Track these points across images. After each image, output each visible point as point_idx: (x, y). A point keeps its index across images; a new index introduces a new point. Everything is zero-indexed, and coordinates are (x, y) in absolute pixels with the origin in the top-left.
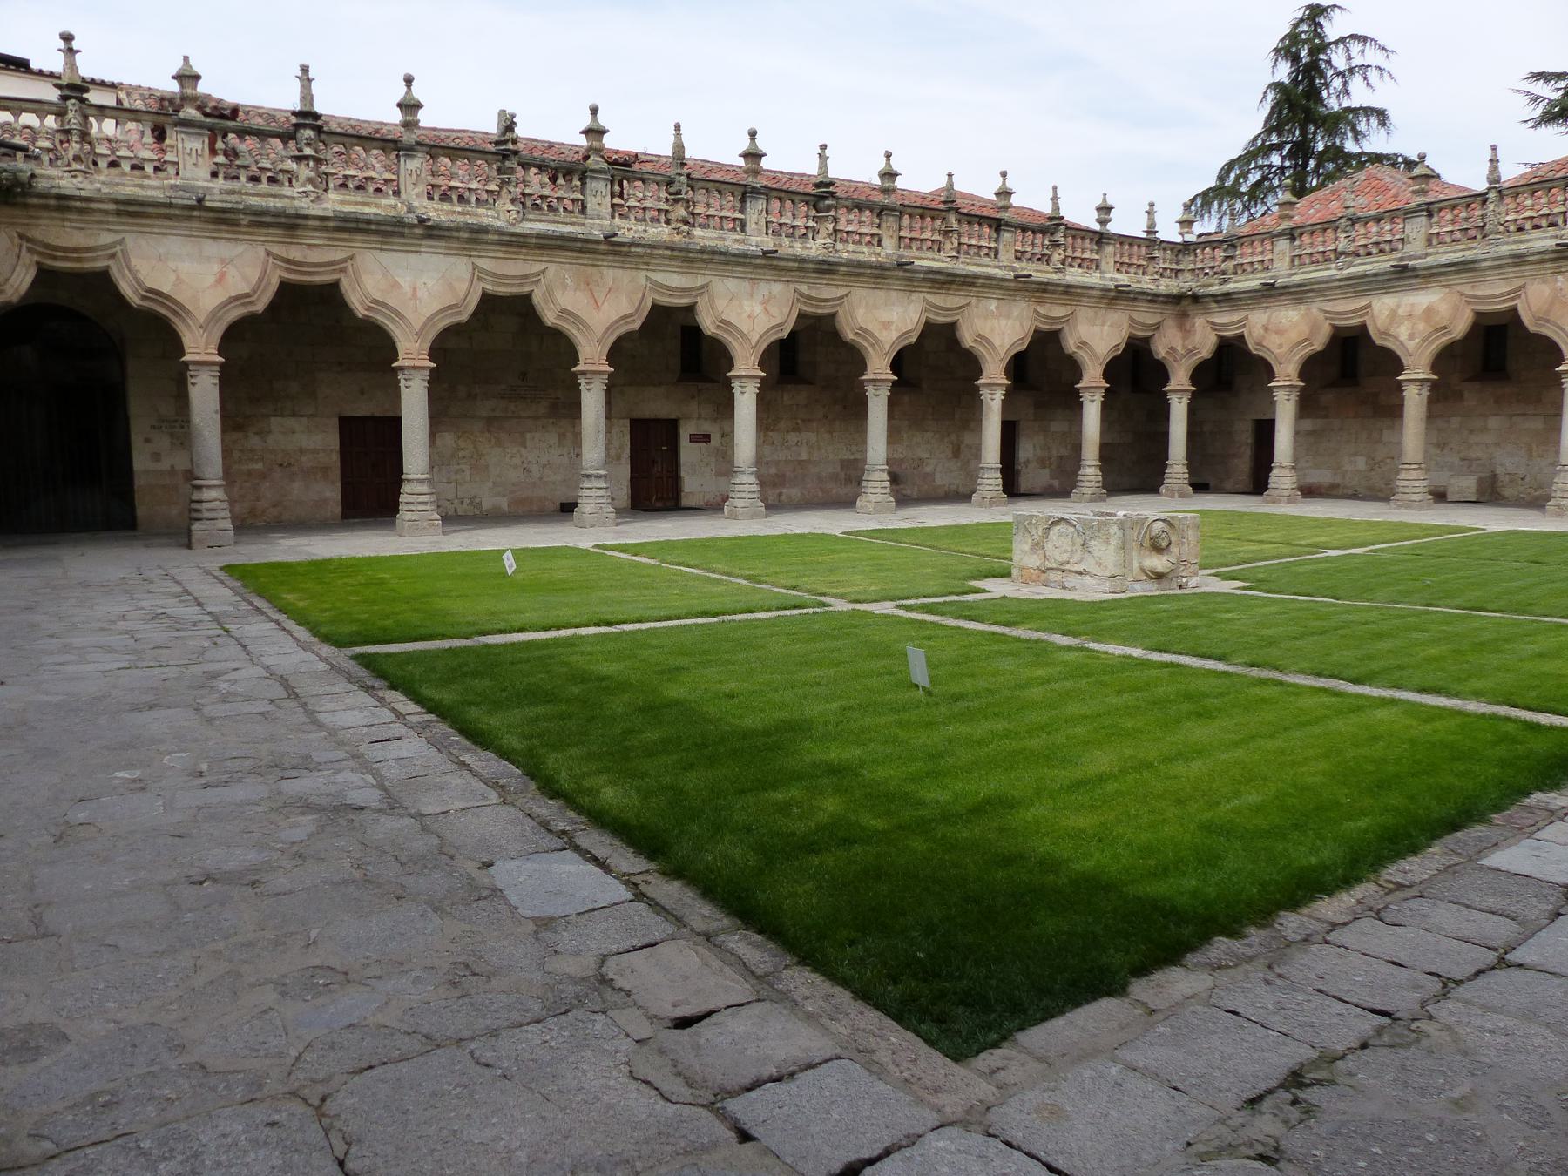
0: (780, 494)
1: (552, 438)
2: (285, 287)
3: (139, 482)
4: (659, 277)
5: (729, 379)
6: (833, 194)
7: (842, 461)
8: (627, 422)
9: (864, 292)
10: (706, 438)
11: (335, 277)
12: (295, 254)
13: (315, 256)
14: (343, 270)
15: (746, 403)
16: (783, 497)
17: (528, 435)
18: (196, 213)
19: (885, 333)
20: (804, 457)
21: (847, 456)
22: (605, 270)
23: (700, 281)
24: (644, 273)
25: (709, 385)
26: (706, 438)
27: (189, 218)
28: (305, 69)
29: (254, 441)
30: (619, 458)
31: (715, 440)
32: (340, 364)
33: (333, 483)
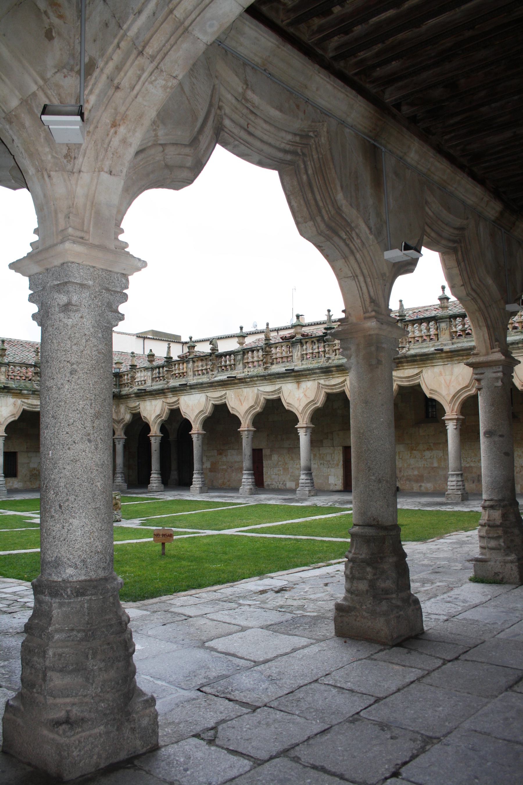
0: (421, 486)
4: (262, 388)
5: (444, 420)
8: (341, 448)
14: (179, 403)
15: (304, 438)
16: (423, 488)
20: (436, 465)
23: (277, 387)
24: (256, 388)
29: (224, 459)
30: (338, 465)
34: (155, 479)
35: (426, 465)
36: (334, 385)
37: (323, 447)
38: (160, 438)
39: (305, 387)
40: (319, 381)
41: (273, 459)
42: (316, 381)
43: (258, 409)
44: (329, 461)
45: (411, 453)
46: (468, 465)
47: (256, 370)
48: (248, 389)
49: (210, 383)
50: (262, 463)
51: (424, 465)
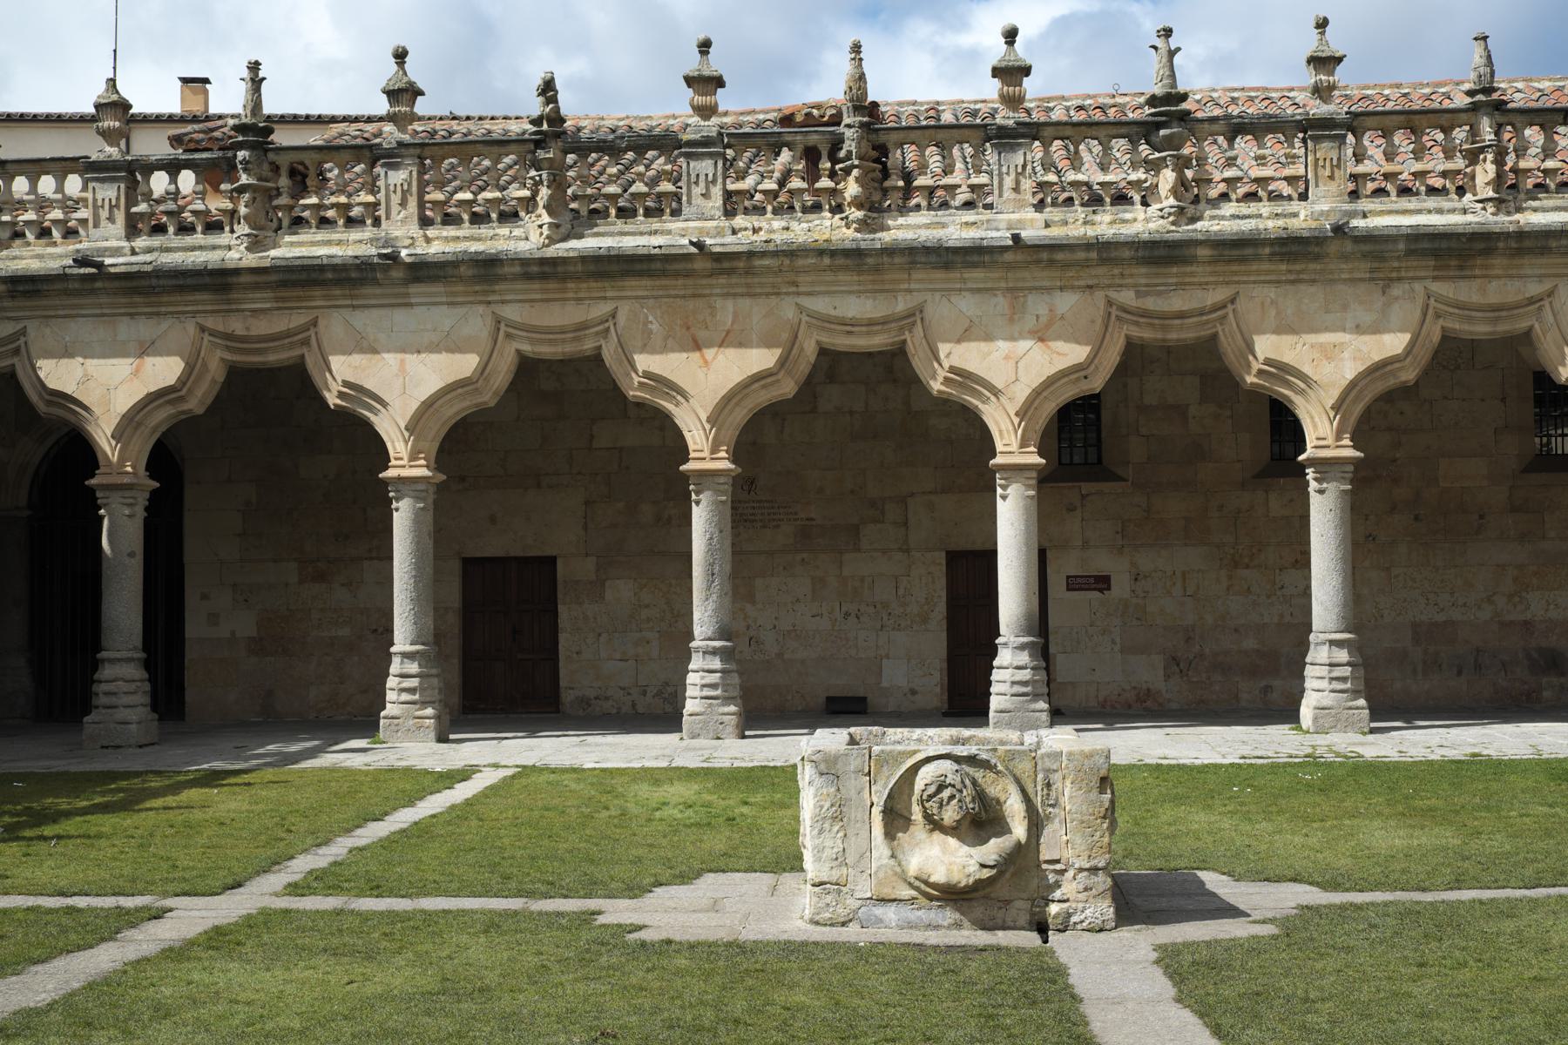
0: (1267, 689)
2: (235, 374)
3: (191, 654)
4: (820, 305)
6: (1184, 117)
8: (941, 557)
9: (1271, 292)
10: (1102, 583)
11: (296, 352)
12: (237, 326)
13: (261, 327)
14: (306, 342)
18: (99, 284)
22: (719, 303)
23: (901, 305)
24: (790, 300)
25: (1106, 486)
26: (1102, 583)
27: (93, 292)
28: (254, 67)
34: (133, 687)
35: (1287, 619)
36: (1181, 315)
38: (142, 500)
39: (1043, 311)
40: (1113, 294)
41: (609, 595)
42: (1100, 295)
45: (1230, 577)
48: (745, 303)
50: (555, 613)
51: (1282, 616)
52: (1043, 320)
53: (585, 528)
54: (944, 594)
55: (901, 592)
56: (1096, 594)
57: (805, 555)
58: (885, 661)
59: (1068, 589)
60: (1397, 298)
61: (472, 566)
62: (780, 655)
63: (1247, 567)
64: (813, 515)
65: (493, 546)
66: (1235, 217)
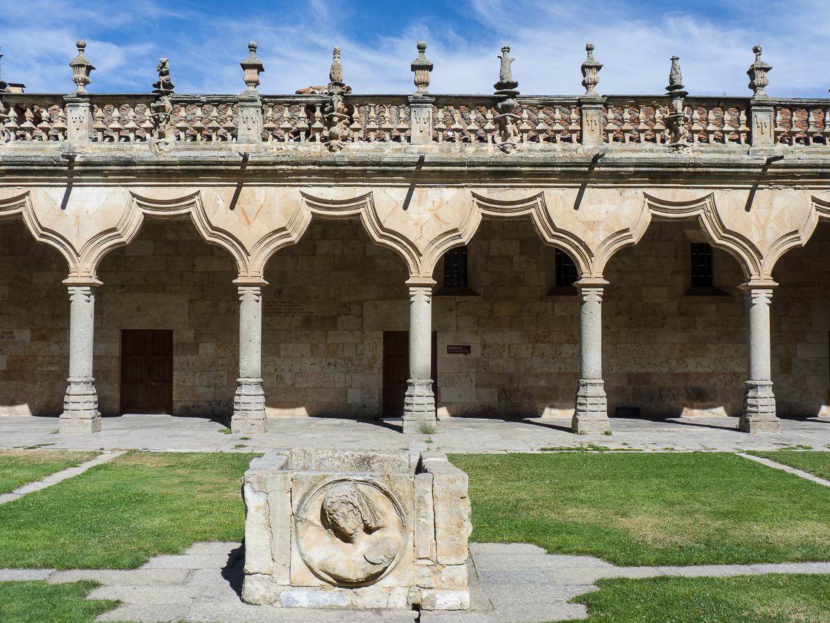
1: (305, 349)
7: (629, 375)
8: (381, 334)
10: (466, 349)
17: (282, 346)
19: (590, 234)
21: (635, 369)
23: (358, 192)
26: (466, 349)
30: (371, 368)
31: (476, 352)
32: (123, 286)
33: (112, 384)
35: (563, 370)
37: (335, 329)
39: (437, 199)
40: (475, 190)
41: (201, 351)
43: (295, 237)
44: (350, 360)
45: (533, 348)
46: (642, 371)
47: (301, 149)
49: (158, 164)
50: (171, 361)
51: (560, 369)
52: (436, 204)
53: (189, 314)
54: (381, 354)
55: (359, 352)
56: (463, 355)
57: (308, 332)
58: (349, 390)
59: (448, 353)
60: (628, 198)
61: (128, 337)
62: (293, 385)
63: (543, 342)
64: (312, 310)
65: (139, 324)
66: (542, 150)
